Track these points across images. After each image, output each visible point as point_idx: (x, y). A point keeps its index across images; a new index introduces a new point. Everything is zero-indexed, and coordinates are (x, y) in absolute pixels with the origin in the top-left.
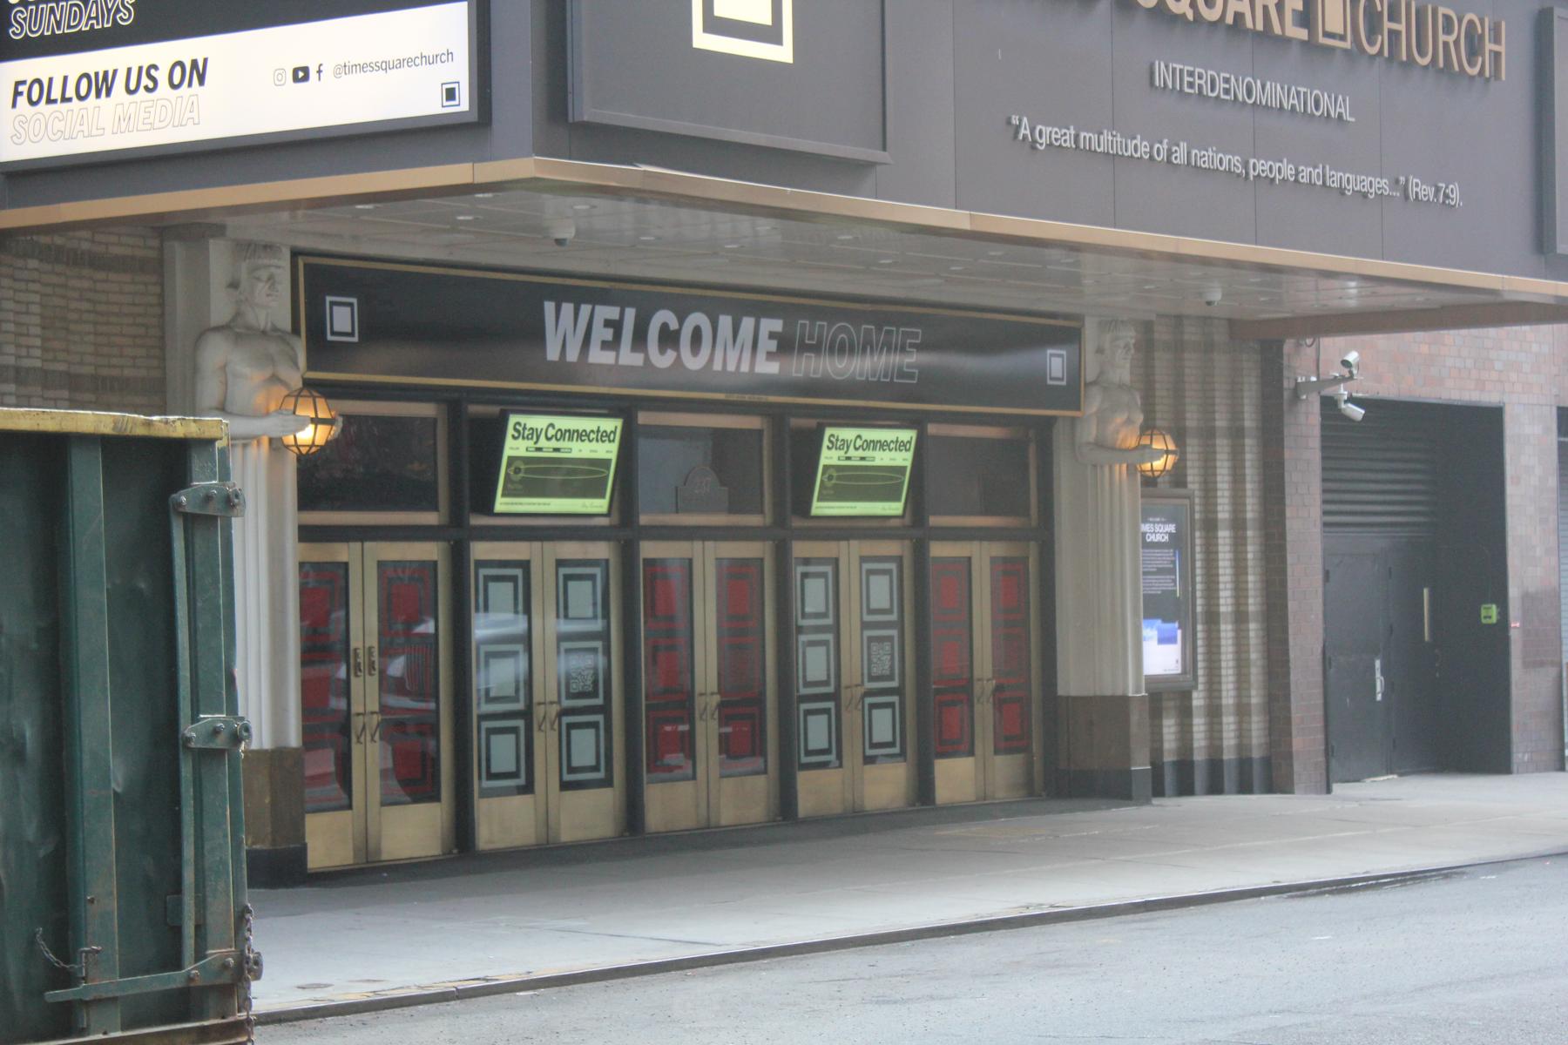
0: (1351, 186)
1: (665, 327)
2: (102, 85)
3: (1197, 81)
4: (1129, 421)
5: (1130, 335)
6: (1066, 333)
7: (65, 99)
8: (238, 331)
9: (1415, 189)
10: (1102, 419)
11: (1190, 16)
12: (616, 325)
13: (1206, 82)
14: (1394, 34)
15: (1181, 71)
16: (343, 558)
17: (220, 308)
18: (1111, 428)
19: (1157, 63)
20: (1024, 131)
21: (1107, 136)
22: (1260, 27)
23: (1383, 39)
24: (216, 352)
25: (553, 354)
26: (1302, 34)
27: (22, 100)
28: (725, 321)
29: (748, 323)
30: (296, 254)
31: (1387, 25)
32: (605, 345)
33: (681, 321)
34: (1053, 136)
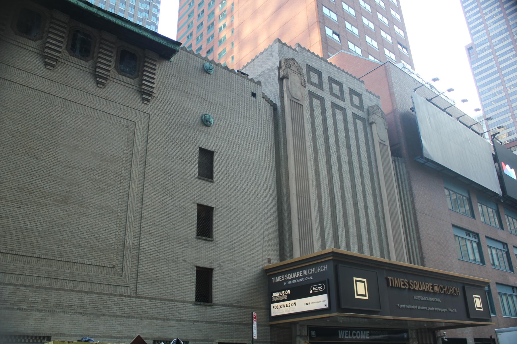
1: (354, 333)
2: (284, 306)
4: (416, 343)
5: (415, 331)
6: (406, 331)
7: (279, 308)
8: (301, 336)
14: (445, 290)
17: (298, 333)
20: (398, 306)
21: (409, 306)
23: (443, 291)
24: (298, 339)
25: (340, 337)
26: (433, 291)
27: (274, 308)
28: (362, 332)
29: (365, 332)
30: (307, 326)
31: (443, 289)
33: (356, 332)
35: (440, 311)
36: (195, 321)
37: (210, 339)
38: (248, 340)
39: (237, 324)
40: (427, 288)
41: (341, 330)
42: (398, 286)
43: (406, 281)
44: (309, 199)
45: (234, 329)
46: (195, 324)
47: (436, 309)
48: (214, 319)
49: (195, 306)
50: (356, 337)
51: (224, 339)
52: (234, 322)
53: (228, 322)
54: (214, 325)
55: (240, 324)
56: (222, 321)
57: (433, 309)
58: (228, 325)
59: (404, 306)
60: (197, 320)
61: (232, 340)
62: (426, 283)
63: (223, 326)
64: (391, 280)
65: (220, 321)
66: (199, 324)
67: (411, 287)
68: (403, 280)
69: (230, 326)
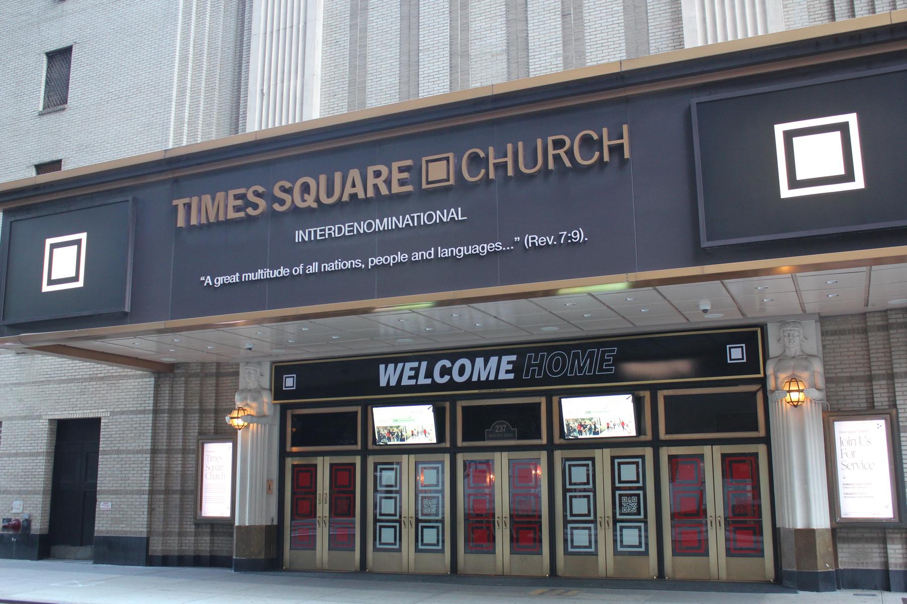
0: (462, 253)
1: (443, 367)
3: (327, 232)
9: (530, 241)
10: (776, 378)
11: (315, 205)
12: (417, 370)
13: (334, 231)
15: (315, 232)
16: (314, 462)
18: (779, 381)
19: (297, 232)
22: (371, 193)
25: (383, 383)
30: (273, 363)
32: (410, 378)
33: (453, 364)
34: (225, 280)
35: (453, 257)
36: (13, 384)
37: (35, 414)
38: (104, 410)
39: (85, 380)
40: (376, 187)
41: (387, 362)
42: (212, 220)
43: (257, 194)
44: (305, 23)
45: (79, 390)
46: (13, 389)
47: (417, 256)
48: (45, 376)
49: (17, 358)
50: (452, 378)
51: (60, 413)
52: (81, 377)
53: (69, 377)
54: (44, 387)
55: (91, 379)
56: (59, 378)
57: (401, 257)
58: (69, 385)
59: (235, 278)
60: (18, 381)
61: (74, 412)
62: (371, 170)
63: (60, 387)
64: (188, 206)
65: (55, 379)
66: (20, 388)
67: (277, 207)
68: (242, 191)
69: (73, 385)
